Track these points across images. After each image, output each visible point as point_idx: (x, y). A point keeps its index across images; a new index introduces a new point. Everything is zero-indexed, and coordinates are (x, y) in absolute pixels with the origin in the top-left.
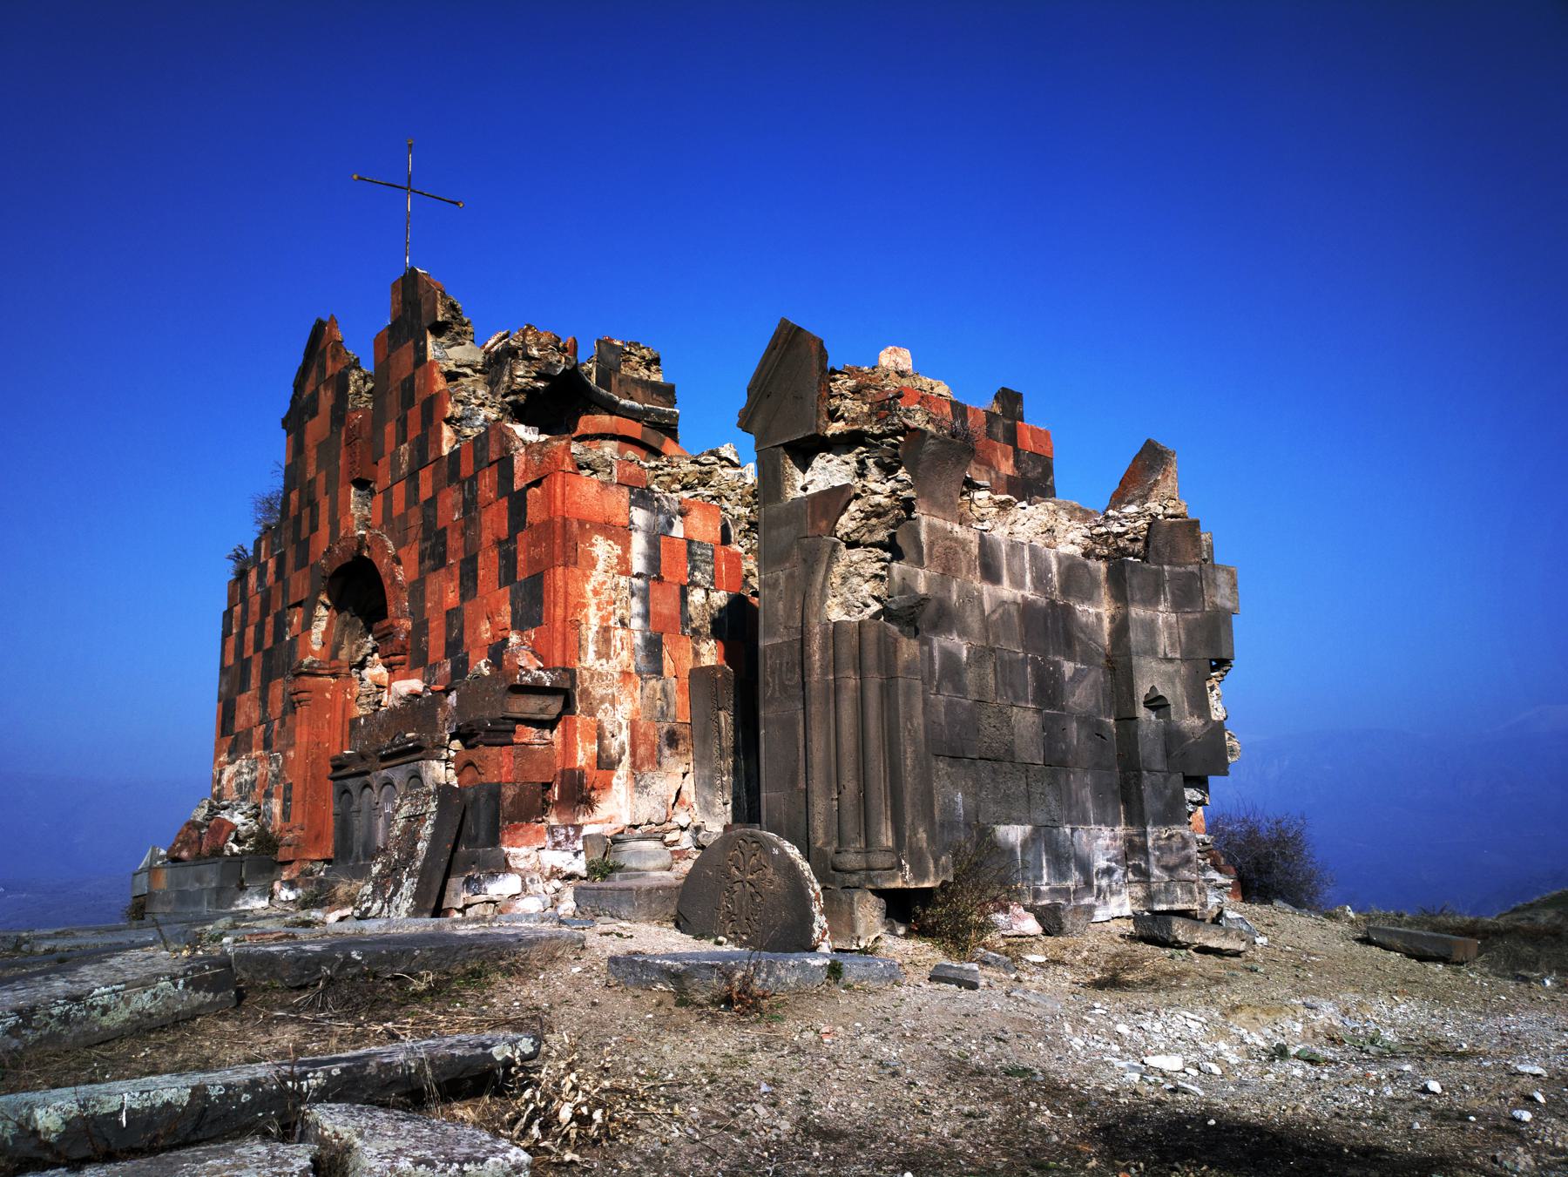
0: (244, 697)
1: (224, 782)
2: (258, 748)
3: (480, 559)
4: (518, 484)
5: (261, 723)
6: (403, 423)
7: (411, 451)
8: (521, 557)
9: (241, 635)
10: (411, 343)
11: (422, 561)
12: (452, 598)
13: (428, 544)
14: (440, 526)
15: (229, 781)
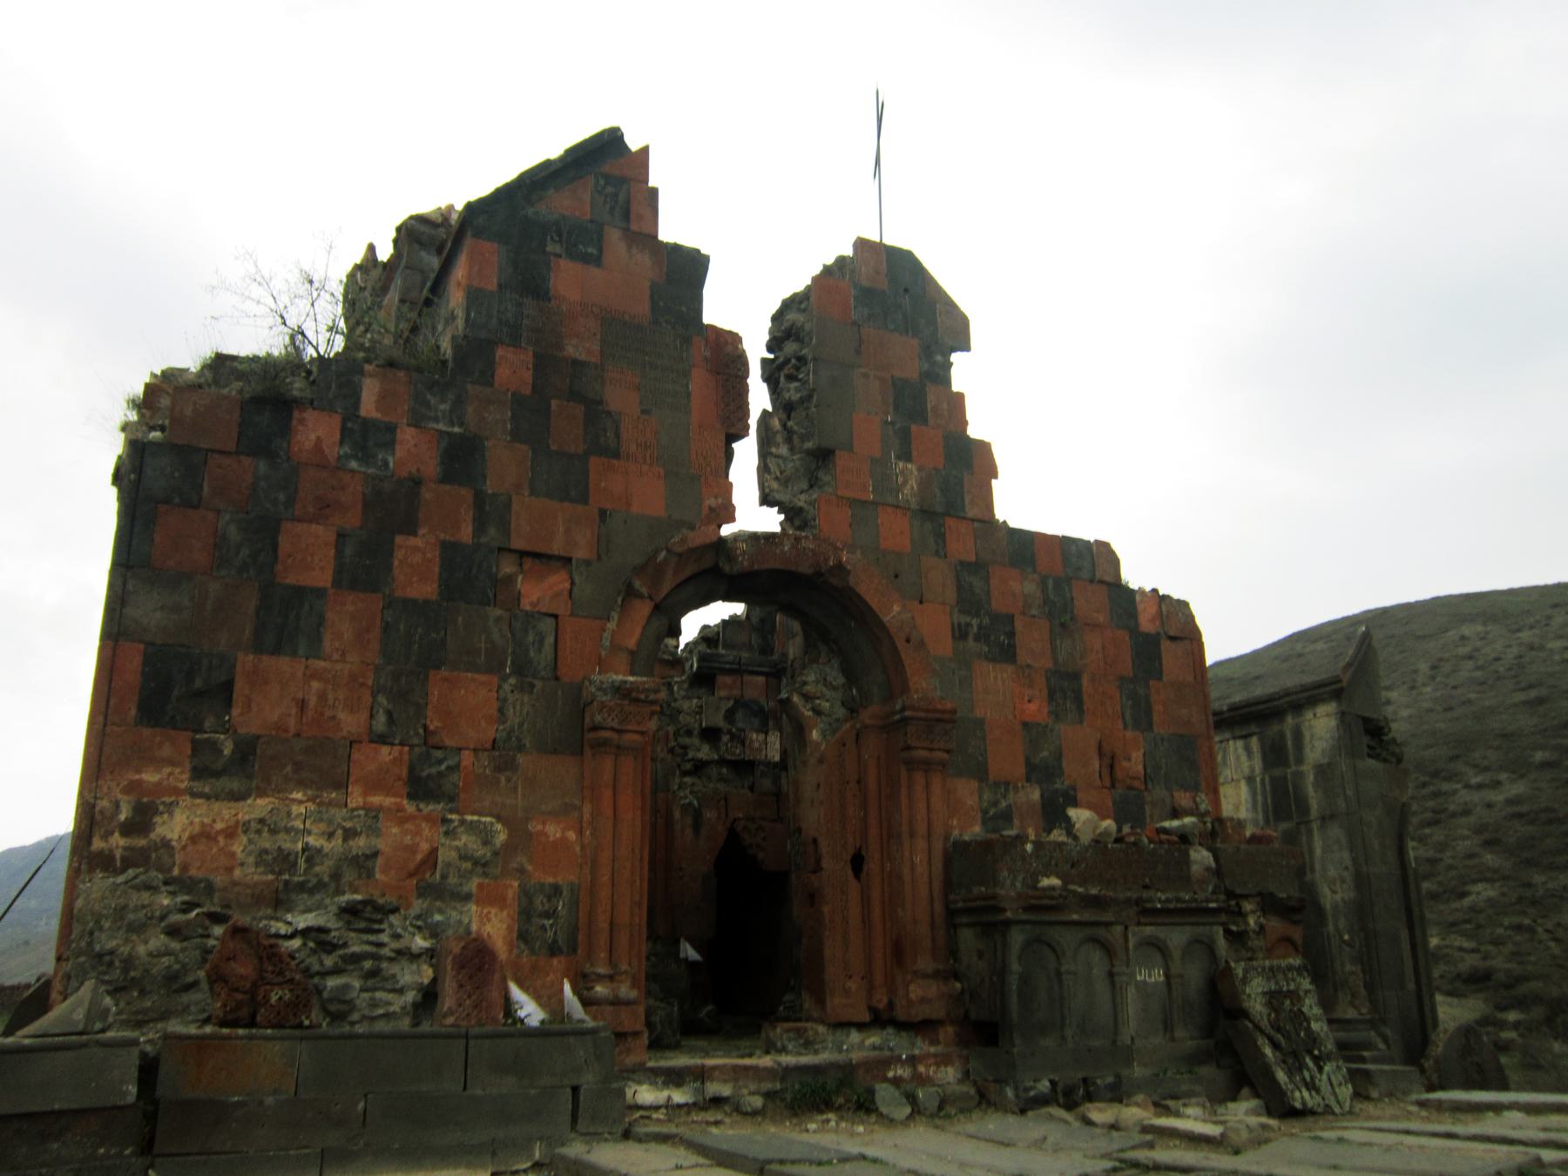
0: (283, 663)
1: (175, 826)
2: (372, 786)
3: (1085, 680)
4: (1146, 624)
5: (382, 739)
6: (905, 437)
7: (924, 484)
8: (1158, 708)
9: (265, 531)
10: (915, 342)
11: (960, 633)
12: (1036, 709)
13: (975, 622)
14: (998, 604)
15: (205, 835)
